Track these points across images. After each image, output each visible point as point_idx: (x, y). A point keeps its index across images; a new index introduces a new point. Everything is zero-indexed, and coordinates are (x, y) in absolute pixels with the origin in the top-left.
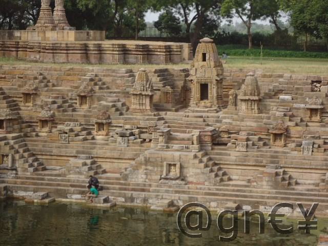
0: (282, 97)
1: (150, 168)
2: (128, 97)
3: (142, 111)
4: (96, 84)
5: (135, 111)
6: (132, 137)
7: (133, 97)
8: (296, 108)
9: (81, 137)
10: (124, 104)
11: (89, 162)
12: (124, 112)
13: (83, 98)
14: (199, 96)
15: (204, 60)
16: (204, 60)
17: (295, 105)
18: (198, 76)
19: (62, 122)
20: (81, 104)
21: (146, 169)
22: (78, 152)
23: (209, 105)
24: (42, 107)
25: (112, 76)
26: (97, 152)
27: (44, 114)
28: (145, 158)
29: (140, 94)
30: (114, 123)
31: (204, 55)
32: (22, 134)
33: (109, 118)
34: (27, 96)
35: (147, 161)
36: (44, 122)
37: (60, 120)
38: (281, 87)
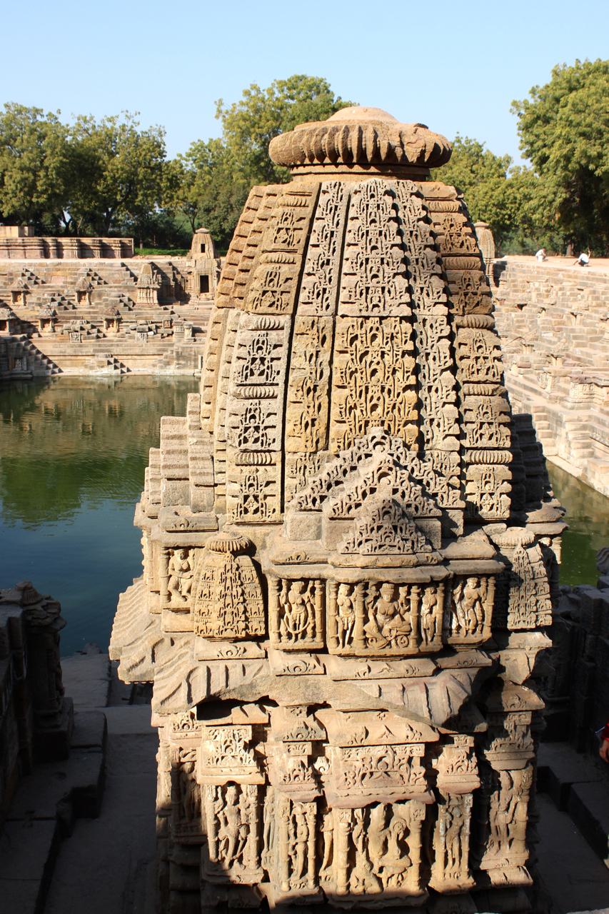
1: (183, 362)
2: (133, 291)
3: (150, 306)
4: (93, 279)
5: (143, 306)
6: (152, 333)
7: (138, 291)
9: (95, 335)
10: (129, 300)
11: (112, 360)
12: (131, 307)
13: (81, 294)
14: (198, 288)
15: (203, 251)
16: (203, 251)
18: (197, 267)
19: (67, 319)
20: (79, 301)
21: (178, 364)
22: (95, 351)
23: (210, 297)
24: (40, 305)
25: (106, 270)
26: (115, 350)
27: (45, 313)
28: (177, 353)
29: (148, 288)
30: (125, 318)
31: (203, 247)
32: (26, 335)
33: (118, 314)
34: (16, 294)
35: (179, 356)
37: (64, 318)
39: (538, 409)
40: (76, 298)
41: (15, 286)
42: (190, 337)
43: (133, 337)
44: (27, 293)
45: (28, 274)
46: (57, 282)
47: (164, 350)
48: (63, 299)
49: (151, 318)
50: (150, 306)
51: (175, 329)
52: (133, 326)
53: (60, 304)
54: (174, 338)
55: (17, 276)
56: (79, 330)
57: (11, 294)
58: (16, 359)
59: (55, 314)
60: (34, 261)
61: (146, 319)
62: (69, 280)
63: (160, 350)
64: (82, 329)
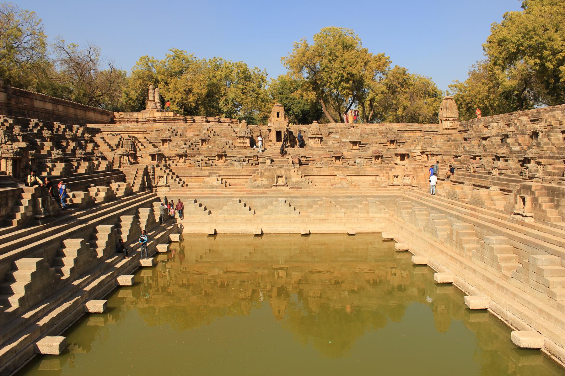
0: (333, 136)
3: (245, 148)
6: (245, 163)
8: (343, 142)
11: (220, 179)
14: (275, 139)
15: (278, 116)
16: (278, 116)
17: (343, 140)
29: (244, 137)
31: (278, 114)
36: (180, 156)
38: (331, 130)
39: (538, 188)
40: (200, 143)
41: (164, 136)
42: (269, 164)
43: (233, 165)
44: (171, 140)
45: (171, 130)
46: (190, 134)
47: (254, 173)
48: (192, 144)
49: (246, 154)
50: (245, 148)
51: (260, 160)
52: (233, 159)
53: (190, 146)
54: (259, 166)
55: (165, 130)
56: (200, 160)
57: (161, 141)
58: (160, 177)
59: (186, 152)
60: (179, 126)
61: (242, 154)
62: (197, 133)
63: (250, 173)
64: (202, 160)
